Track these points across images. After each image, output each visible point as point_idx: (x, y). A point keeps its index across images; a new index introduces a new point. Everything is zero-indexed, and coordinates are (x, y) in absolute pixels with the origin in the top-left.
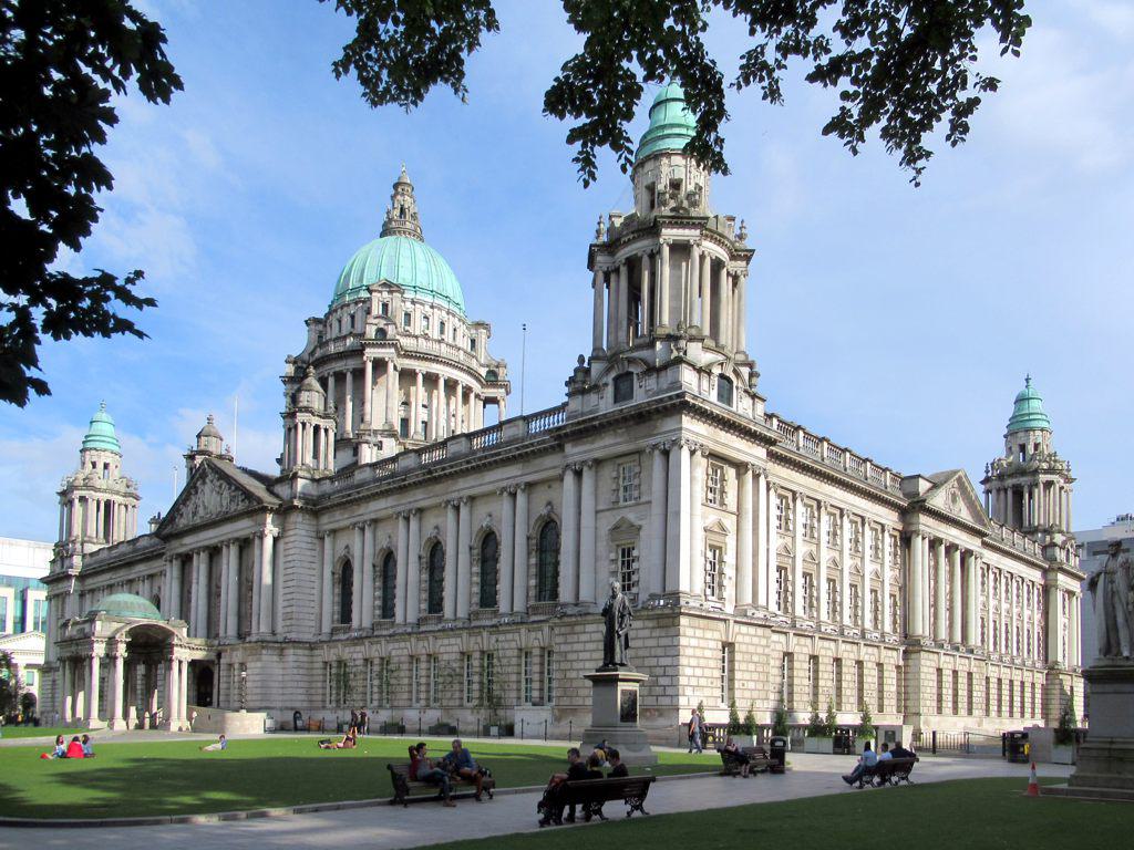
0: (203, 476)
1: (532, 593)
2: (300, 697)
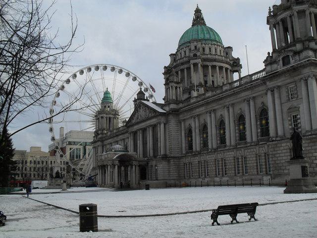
0: (140, 107)
1: (259, 134)
2: (176, 175)
